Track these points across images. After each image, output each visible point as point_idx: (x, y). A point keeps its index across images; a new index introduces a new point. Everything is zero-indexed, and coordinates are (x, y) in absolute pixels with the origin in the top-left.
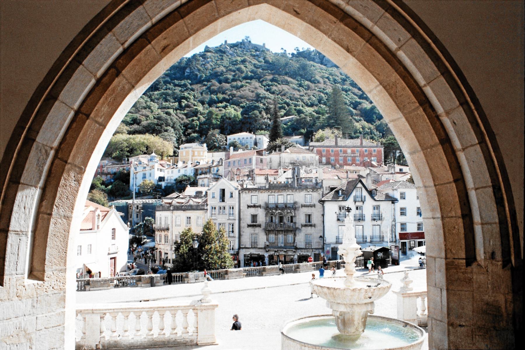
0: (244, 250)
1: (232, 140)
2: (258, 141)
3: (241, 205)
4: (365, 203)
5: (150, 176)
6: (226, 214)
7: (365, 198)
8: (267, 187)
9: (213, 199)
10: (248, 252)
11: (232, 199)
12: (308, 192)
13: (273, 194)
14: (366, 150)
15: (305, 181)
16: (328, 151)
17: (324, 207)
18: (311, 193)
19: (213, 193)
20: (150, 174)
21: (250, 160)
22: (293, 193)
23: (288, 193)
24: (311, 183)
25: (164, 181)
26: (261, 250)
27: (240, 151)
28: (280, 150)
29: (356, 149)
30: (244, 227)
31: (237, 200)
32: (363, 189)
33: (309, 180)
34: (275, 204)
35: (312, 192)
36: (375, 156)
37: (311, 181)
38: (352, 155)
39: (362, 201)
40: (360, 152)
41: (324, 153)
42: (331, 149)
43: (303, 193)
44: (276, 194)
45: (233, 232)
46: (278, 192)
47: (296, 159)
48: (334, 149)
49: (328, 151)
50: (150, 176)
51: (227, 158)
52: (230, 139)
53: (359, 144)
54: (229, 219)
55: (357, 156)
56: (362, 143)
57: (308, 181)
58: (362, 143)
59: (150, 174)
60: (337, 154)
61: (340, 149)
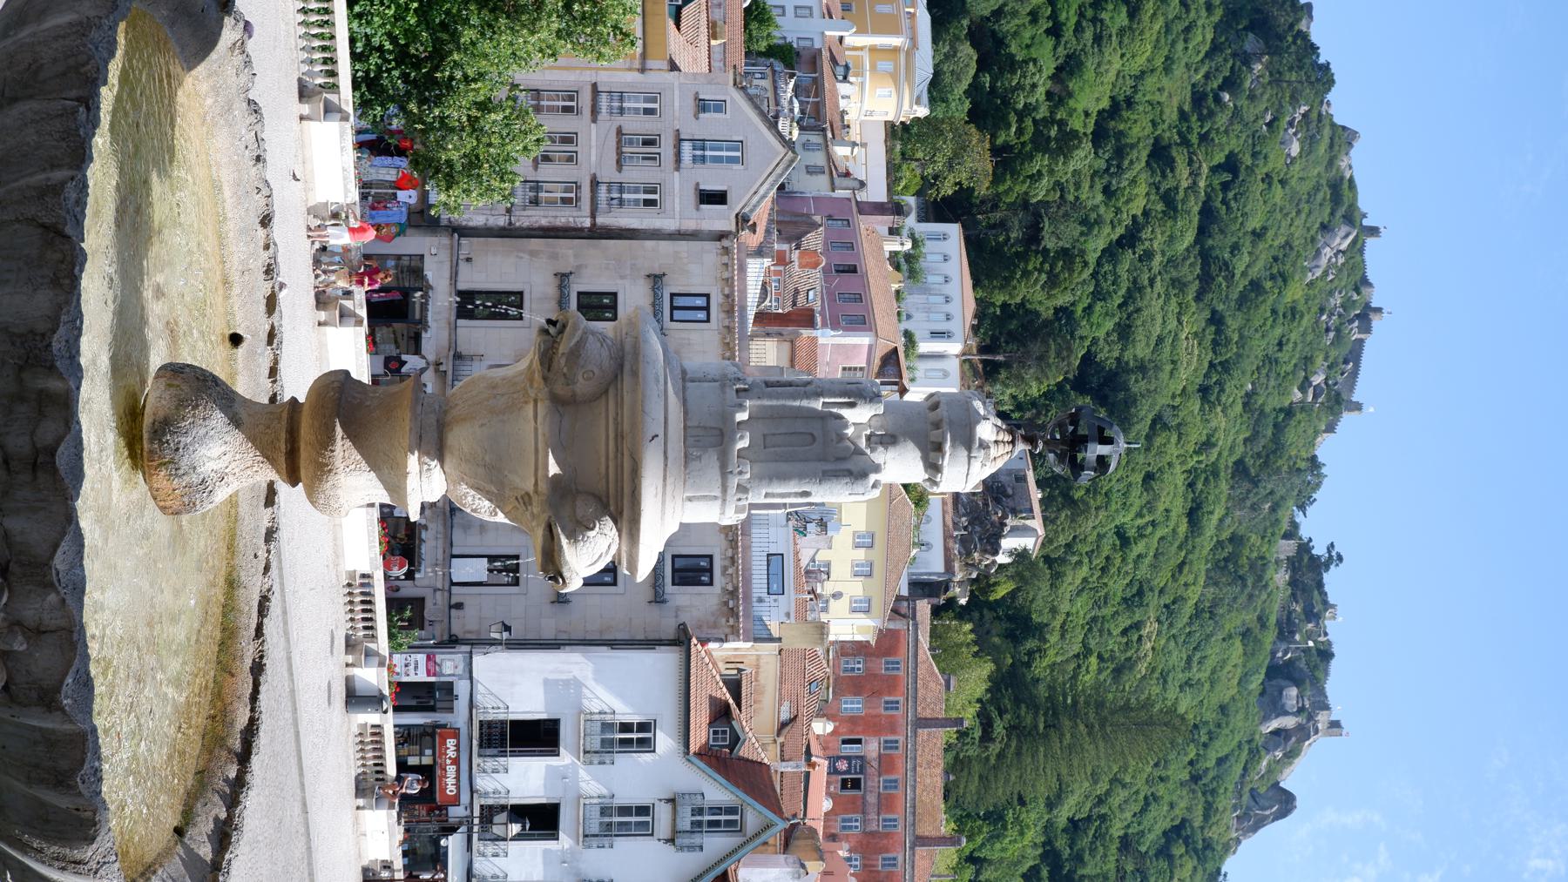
0: (444, 256)
3: (665, 246)
4: (669, 848)
6: (619, 165)
7: (691, 848)
9: (690, 104)
10: (436, 273)
11: (692, 197)
17: (649, 644)
19: (720, 107)
26: (445, 334)
30: (554, 257)
31: (690, 225)
40: (887, 835)
45: (535, 202)
54: (595, 183)
55: (864, 821)
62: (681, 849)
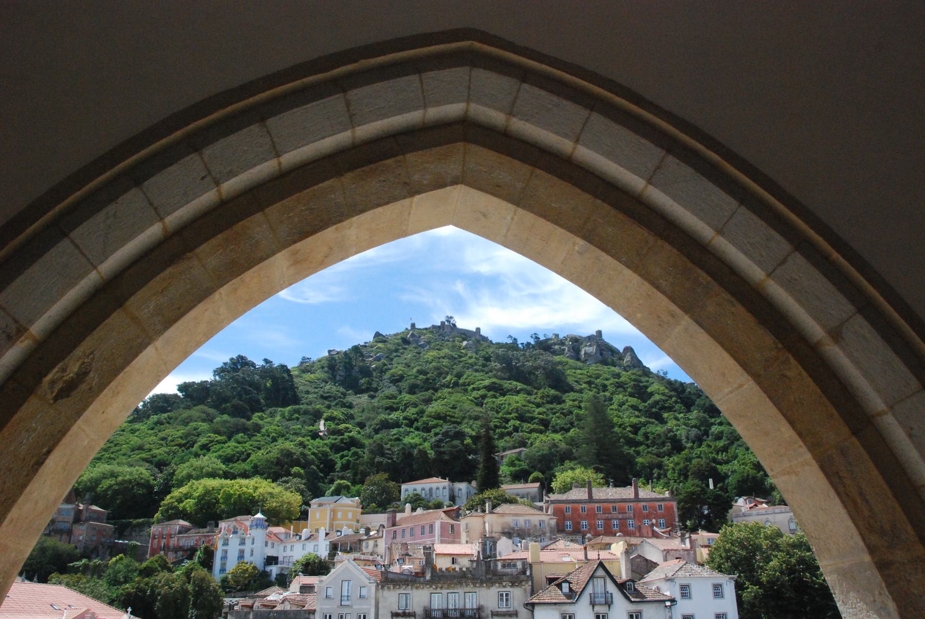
1: (411, 492)
2: (456, 494)
5: (252, 555)
8: (428, 577)
12: (504, 587)
13: (439, 590)
14: (645, 508)
15: (504, 566)
16: (575, 510)
18: (508, 589)
20: (252, 551)
21: (432, 527)
22: (477, 590)
23: (467, 589)
24: (514, 570)
25: (276, 563)
27: (419, 511)
28: (484, 511)
29: (627, 505)
32: (608, 580)
33: (508, 563)
34: (443, 610)
35: (511, 586)
36: (663, 516)
37: (515, 566)
38: (620, 516)
39: (606, 603)
41: (569, 514)
42: (581, 505)
43: (494, 591)
44: (445, 591)
46: (448, 588)
47: (512, 525)
48: (586, 506)
49: (575, 510)
50: (252, 555)
51: (390, 524)
52: (407, 490)
53: (632, 496)
56: (636, 494)
57: (509, 565)
58: (636, 494)
59: (252, 551)
60: (591, 516)
61: (597, 505)
62: (612, 602)
